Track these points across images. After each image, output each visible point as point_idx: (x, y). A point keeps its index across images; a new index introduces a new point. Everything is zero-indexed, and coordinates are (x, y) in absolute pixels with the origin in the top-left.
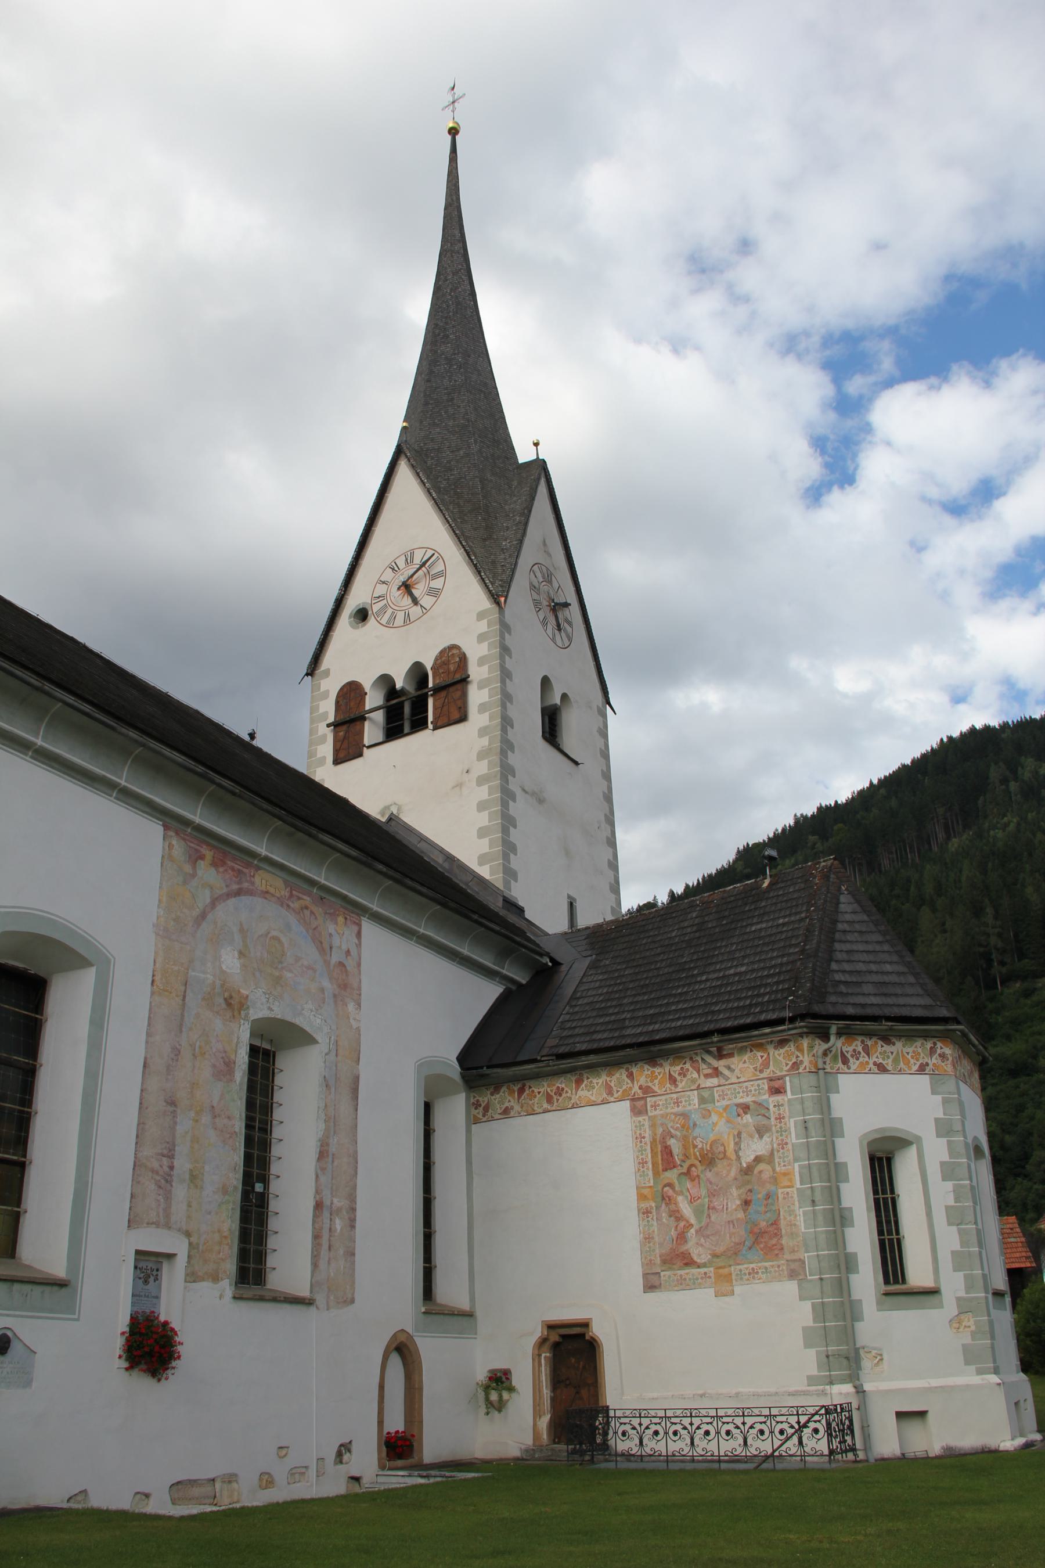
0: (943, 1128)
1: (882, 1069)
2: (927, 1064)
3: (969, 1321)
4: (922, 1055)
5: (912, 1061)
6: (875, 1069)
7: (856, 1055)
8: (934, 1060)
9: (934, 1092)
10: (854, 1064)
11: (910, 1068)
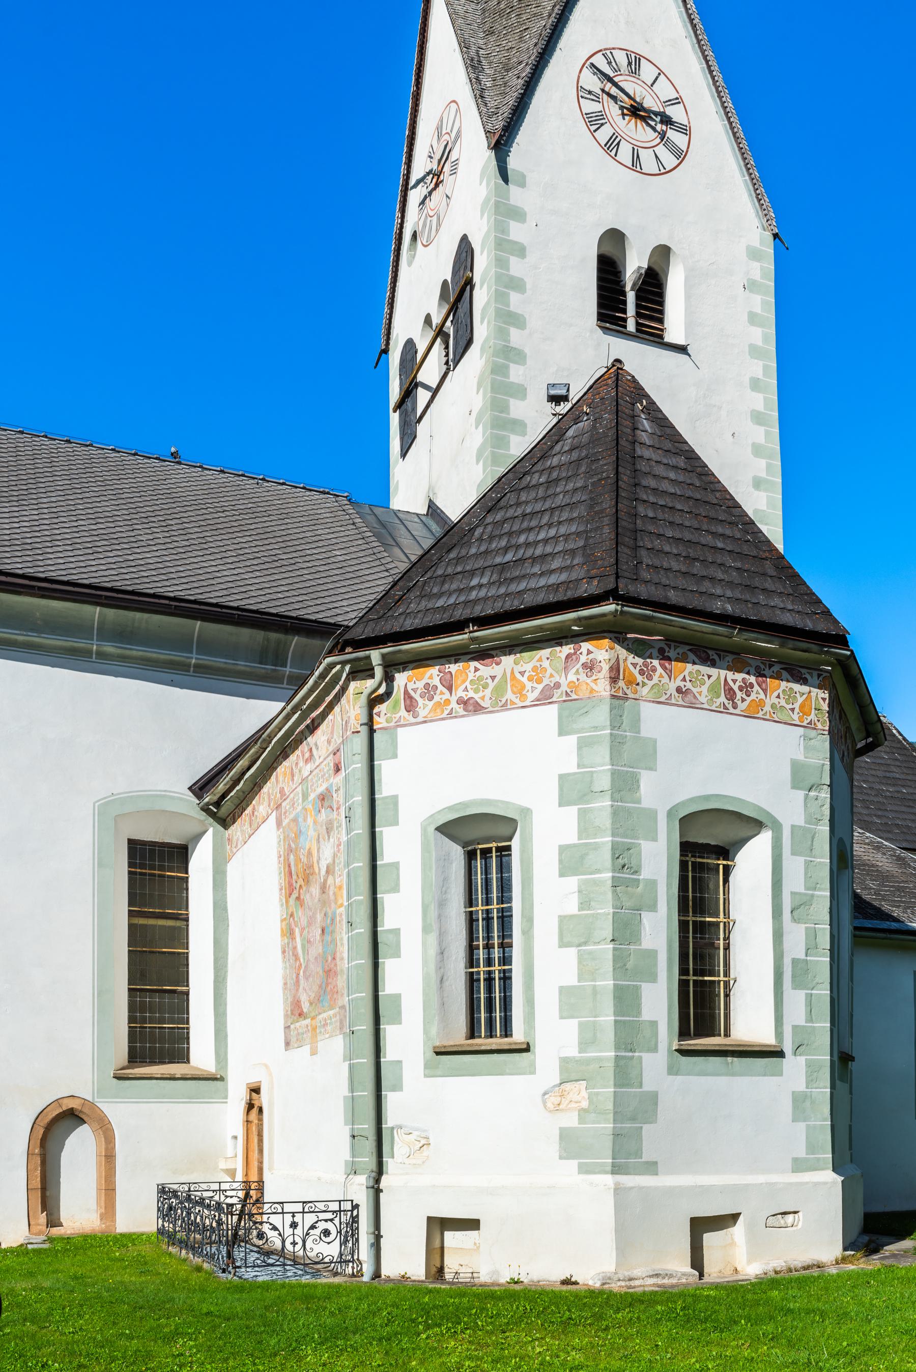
0: (572, 790)
1: (472, 707)
2: (557, 685)
3: (579, 1093)
4: (549, 671)
5: (529, 685)
6: (460, 710)
7: (429, 692)
8: (572, 677)
9: (563, 731)
10: (424, 707)
11: (523, 697)
